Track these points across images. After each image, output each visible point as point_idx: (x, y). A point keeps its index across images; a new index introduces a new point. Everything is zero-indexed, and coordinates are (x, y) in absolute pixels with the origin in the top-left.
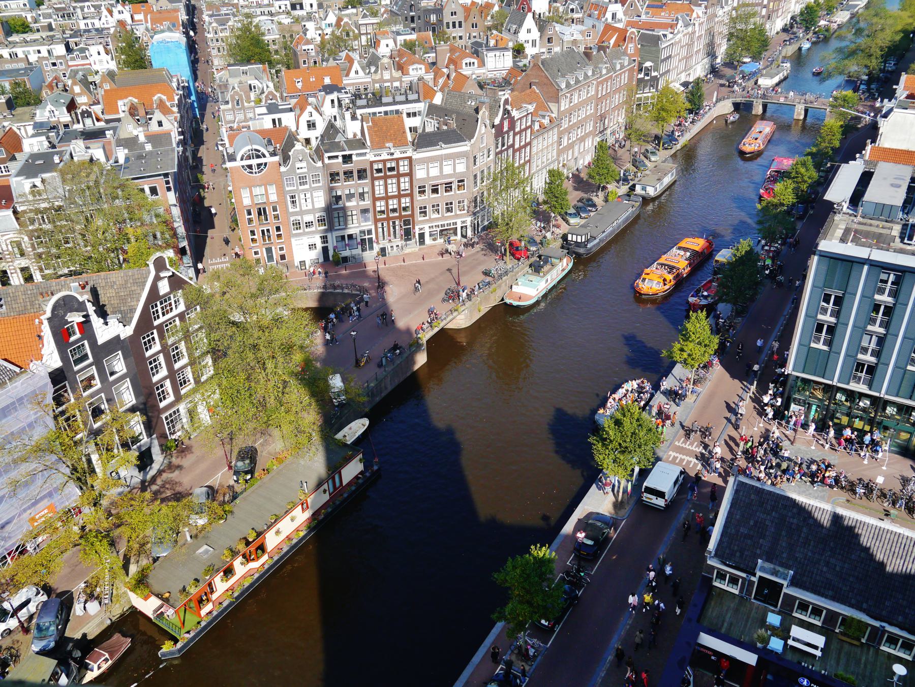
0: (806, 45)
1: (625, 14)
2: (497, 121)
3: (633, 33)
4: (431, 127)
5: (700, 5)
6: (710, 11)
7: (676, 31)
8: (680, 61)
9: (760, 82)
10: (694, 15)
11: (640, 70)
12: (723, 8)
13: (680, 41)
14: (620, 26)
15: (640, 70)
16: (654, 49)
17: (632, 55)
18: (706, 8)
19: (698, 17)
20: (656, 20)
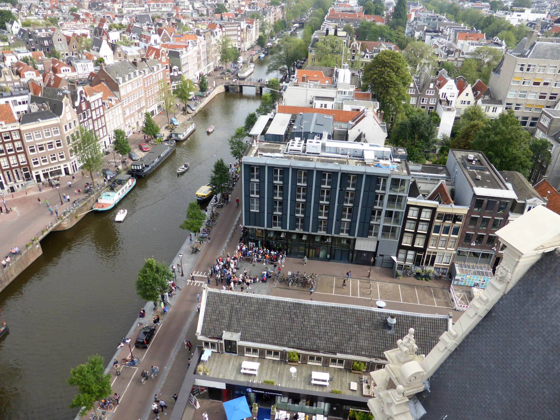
0: (263, 55)
1: (162, 40)
2: (77, 104)
3: (163, 51)
4: (35, 108)
5: (201, 35)
6: (208, 39)
7: (188, 50)
8: (194, 65)
9: (239, 75)
10: (198, 41)
11: (171, 71)
12: (214, 36)
13: (192, 54)
14: (158, 47)
15: (171, 71)
16: (177, 59)
17: (165, 63)
18: (204, 36)
19: (201, 42)
20: (177, 44)
